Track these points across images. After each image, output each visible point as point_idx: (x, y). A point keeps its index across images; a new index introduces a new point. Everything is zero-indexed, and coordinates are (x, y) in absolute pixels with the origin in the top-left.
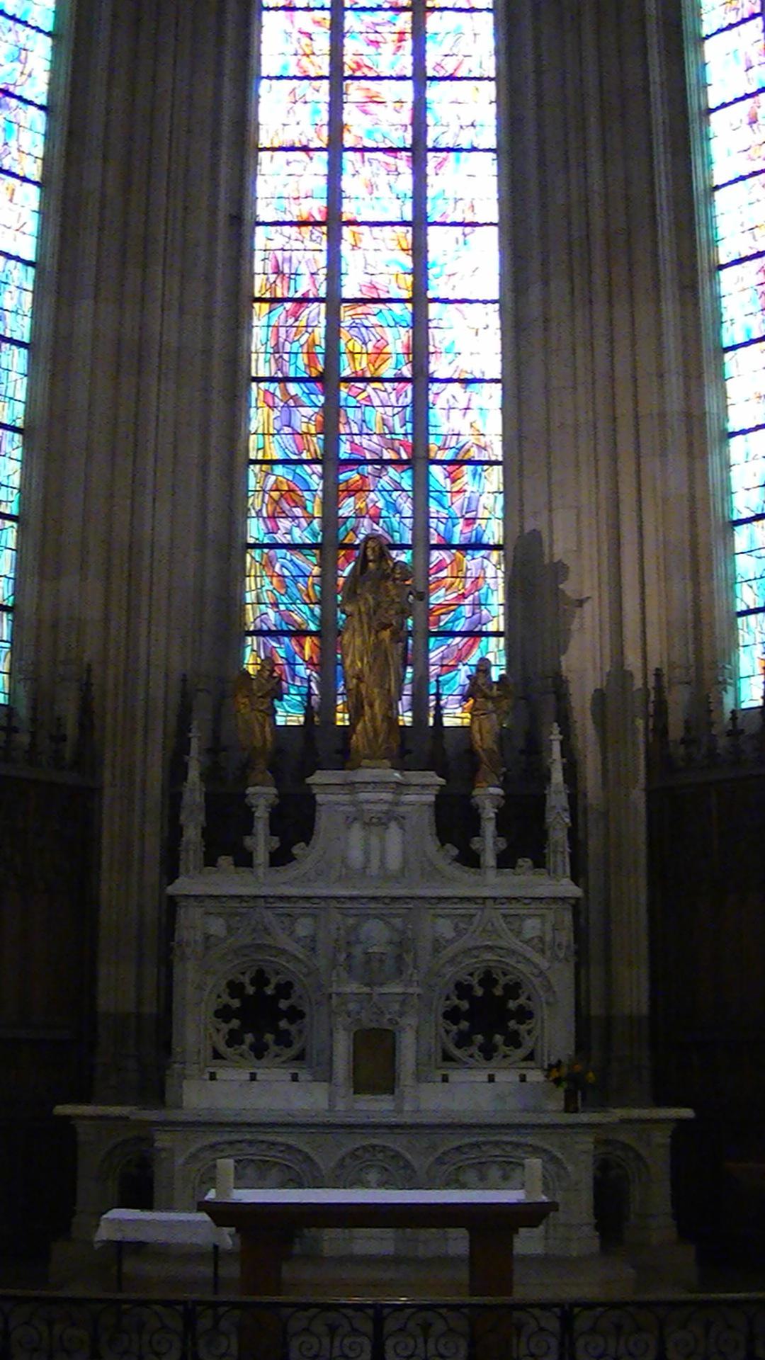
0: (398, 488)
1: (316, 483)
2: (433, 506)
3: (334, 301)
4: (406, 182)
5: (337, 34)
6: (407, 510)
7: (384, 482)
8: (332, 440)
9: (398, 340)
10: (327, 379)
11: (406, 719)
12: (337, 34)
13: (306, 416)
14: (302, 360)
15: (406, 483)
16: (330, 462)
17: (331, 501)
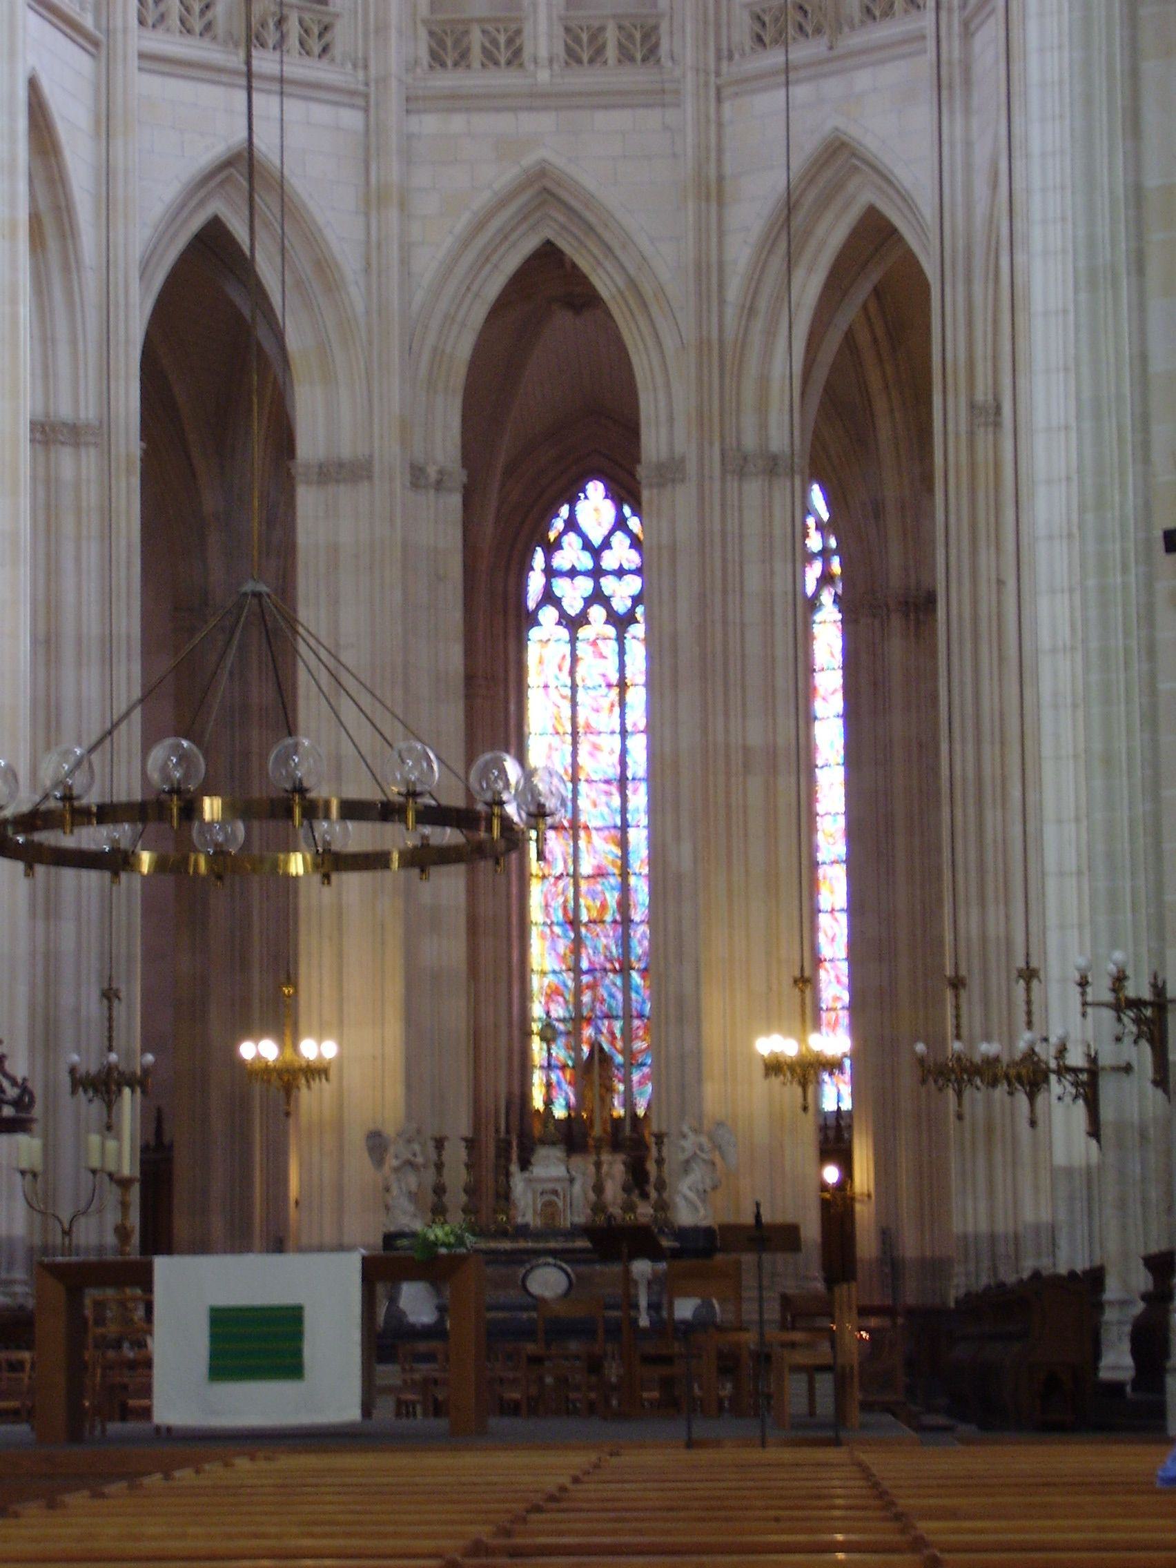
0: (615, 984)
1: (570, 984)
2: (634, 995)
3: (576, 876)
4: (616, 801)
5: (574, 704)
6: (620, 996)
7: (607, 982)
8: (577, 960)
9: (612, 898)
10: (573, 922)
11: (619, 1111)
12: (574, 704)
13: (563, 946)
14: (560, 914)
15: (619, 982)
16: (577, 971)
17: (578, 992)
